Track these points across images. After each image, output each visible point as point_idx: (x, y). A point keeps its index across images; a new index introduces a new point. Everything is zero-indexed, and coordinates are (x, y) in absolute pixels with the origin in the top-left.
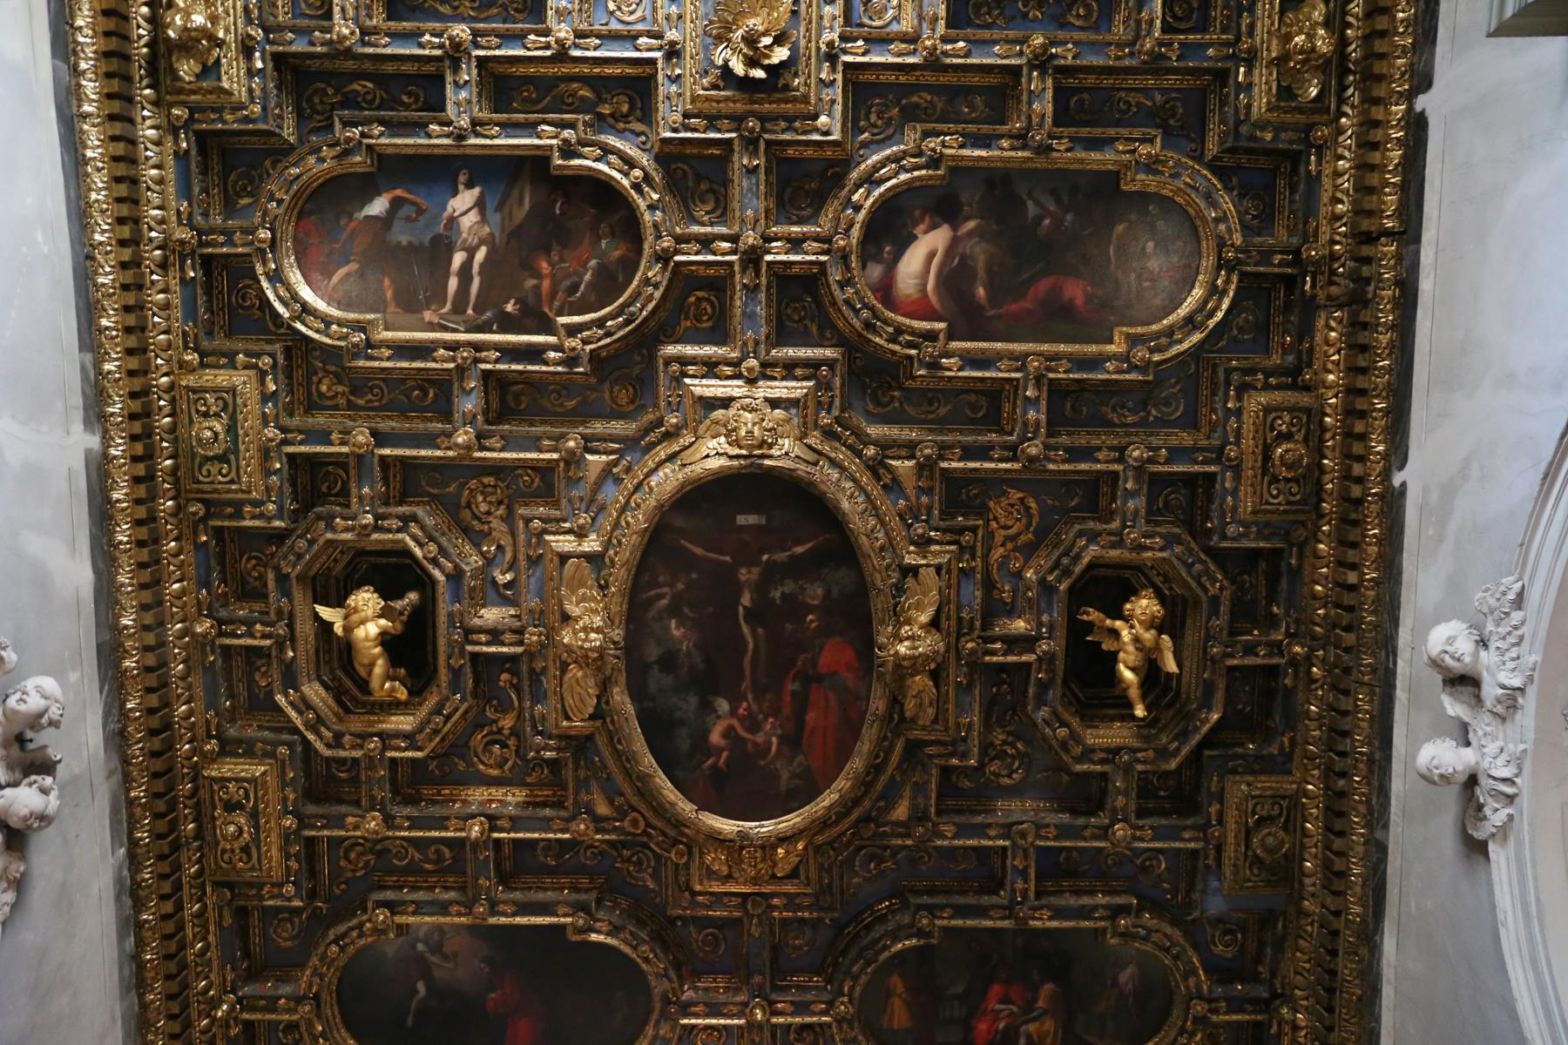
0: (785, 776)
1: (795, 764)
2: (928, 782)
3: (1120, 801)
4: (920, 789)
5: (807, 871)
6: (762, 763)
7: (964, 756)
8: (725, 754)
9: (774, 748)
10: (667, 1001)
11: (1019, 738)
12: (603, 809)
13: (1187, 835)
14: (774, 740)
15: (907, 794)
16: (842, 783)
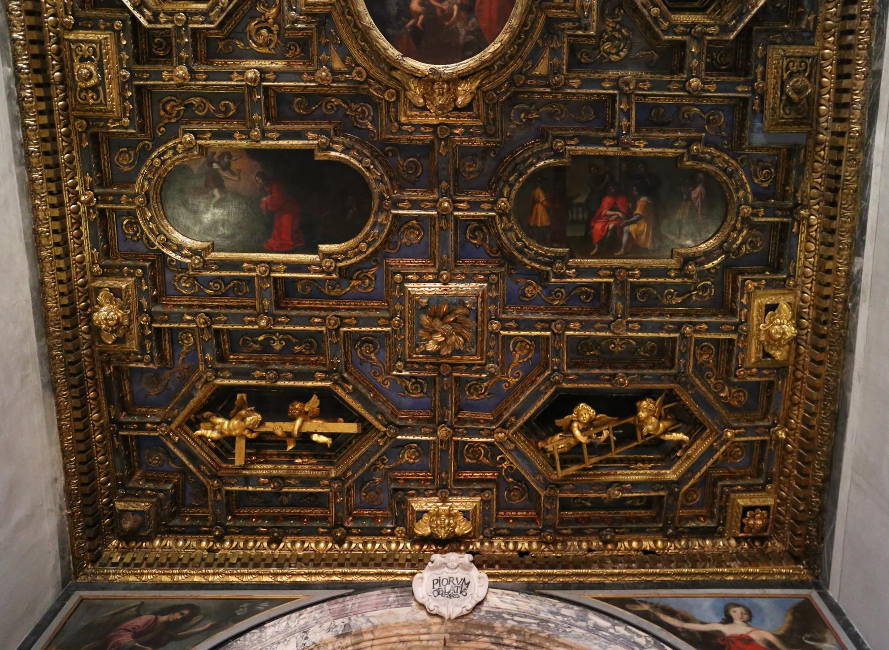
0: (463, 32)
1: (470, 25)
2: (562, 48)
3: (695, 62)
4: (555, 52)
5: (478, 106)
6: (447, 23)
7: (586, 29)
8: (421, 17)
9: (455, 13)
10: (382, 198)
11: (623, 26)
12: (337, 65)
13: (739, 89)
14: (455, 7)
15: (546, 54)
16: (503, 36)
